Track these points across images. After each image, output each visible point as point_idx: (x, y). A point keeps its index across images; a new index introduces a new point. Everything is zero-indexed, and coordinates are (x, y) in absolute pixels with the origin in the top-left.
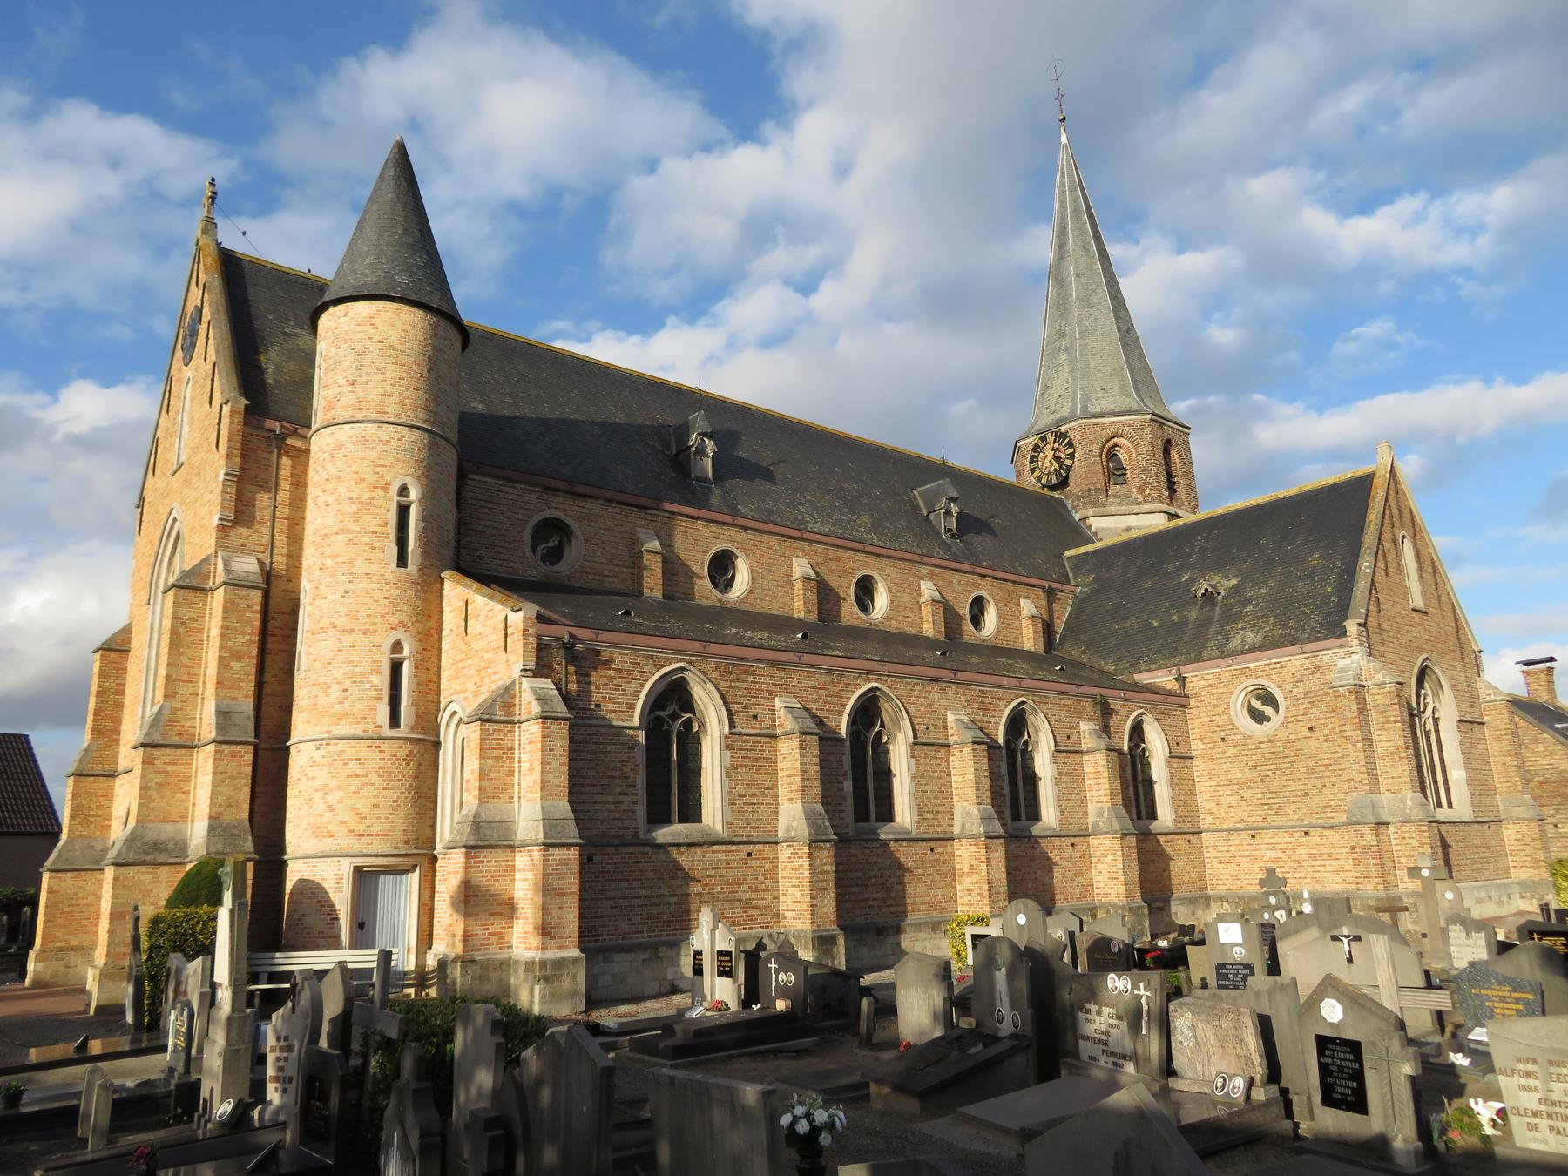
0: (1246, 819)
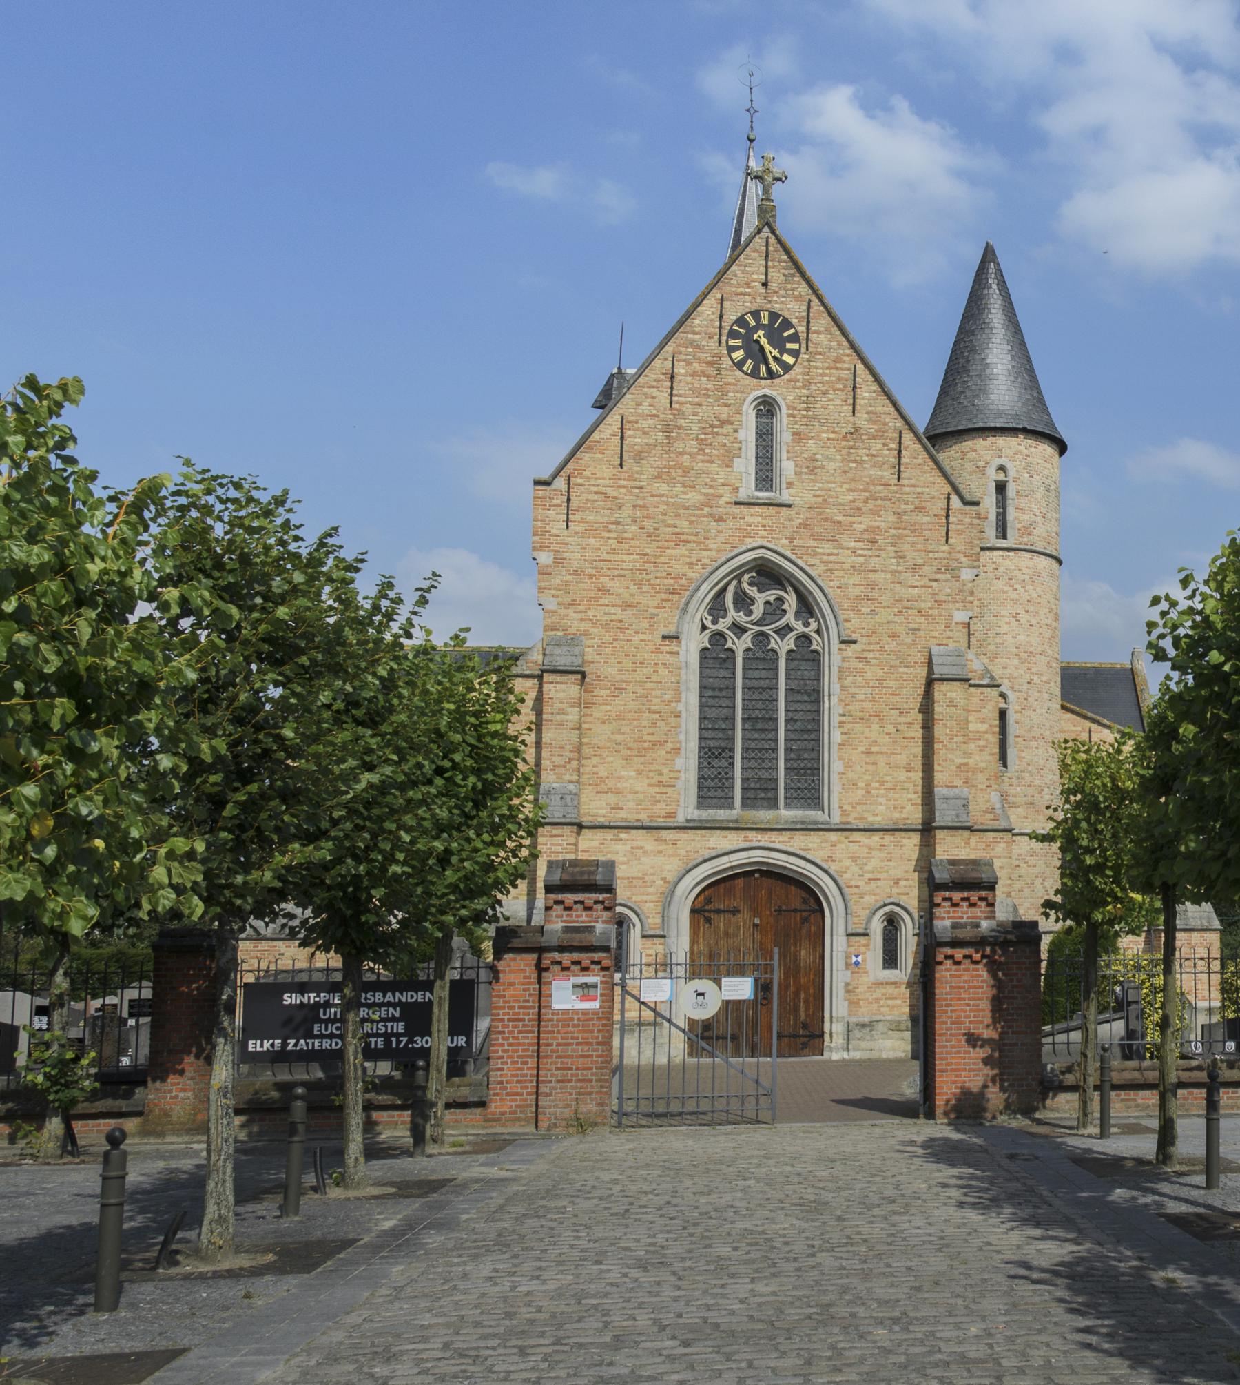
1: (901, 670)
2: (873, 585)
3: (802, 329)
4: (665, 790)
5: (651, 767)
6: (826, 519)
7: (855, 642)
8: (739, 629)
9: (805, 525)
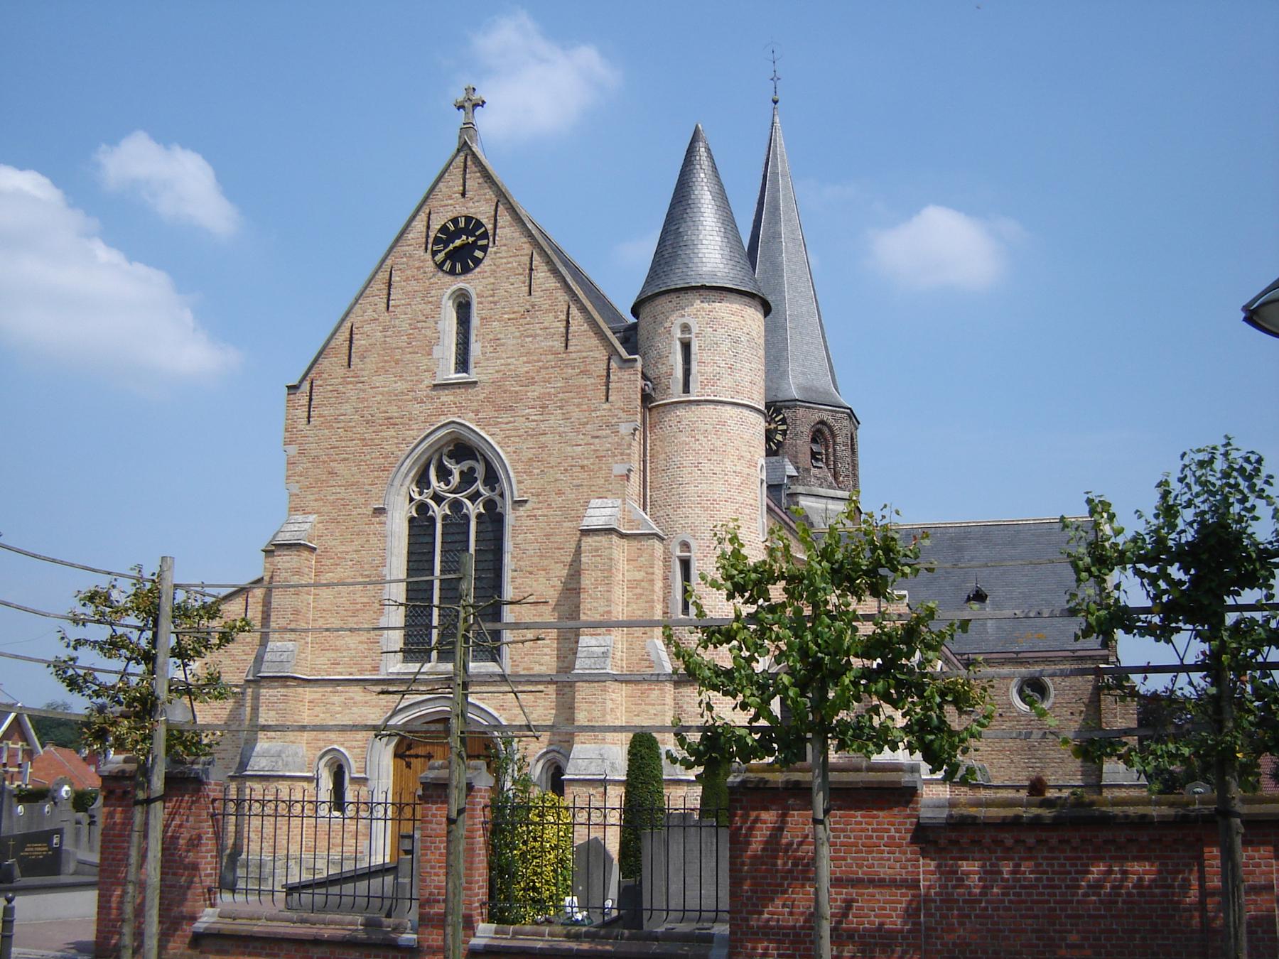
0: (1014, 778)
1: (565, 524)
2: (543, 447)
3: (490, 227)
6: (505, 392)
8: (438, 499)
9: (488, 399)
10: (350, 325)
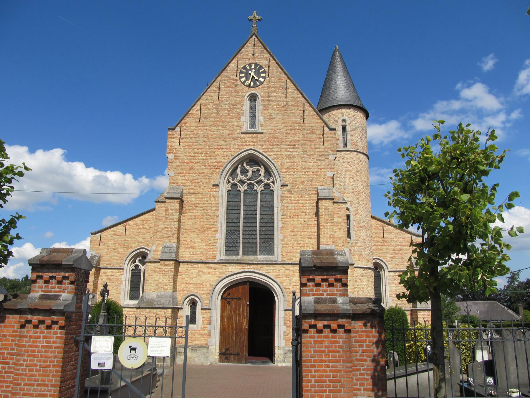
1: (306, 196)
2: (294, 163)
3: (266, 69)
4: (212, 247)
5: (207, 238)
6: (276, 138)
7: (287, 185)
8: (242, 182)
9: (267, 140)
10: (200, 104)
